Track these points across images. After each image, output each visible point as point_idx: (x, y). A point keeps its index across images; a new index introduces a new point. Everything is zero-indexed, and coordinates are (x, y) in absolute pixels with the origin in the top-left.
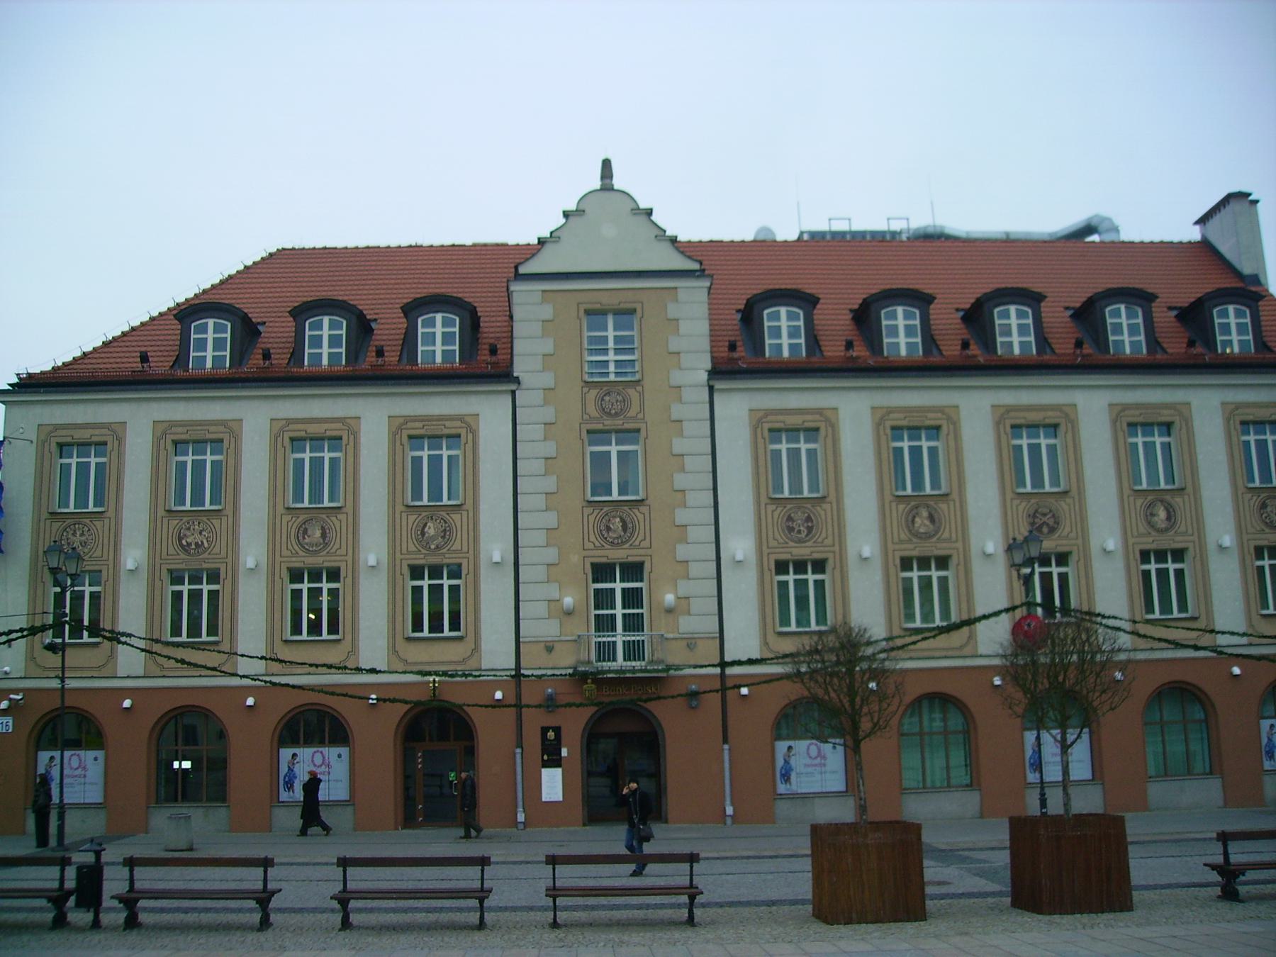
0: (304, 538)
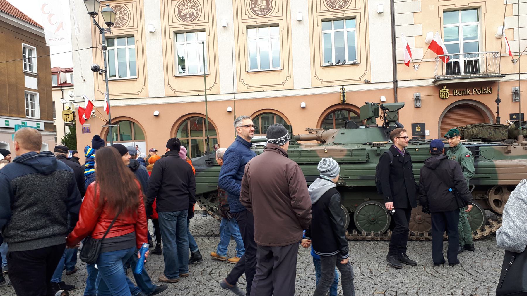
0: (256, 7)
